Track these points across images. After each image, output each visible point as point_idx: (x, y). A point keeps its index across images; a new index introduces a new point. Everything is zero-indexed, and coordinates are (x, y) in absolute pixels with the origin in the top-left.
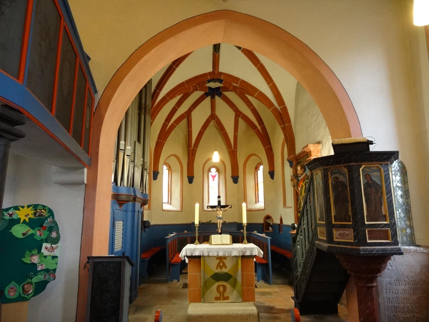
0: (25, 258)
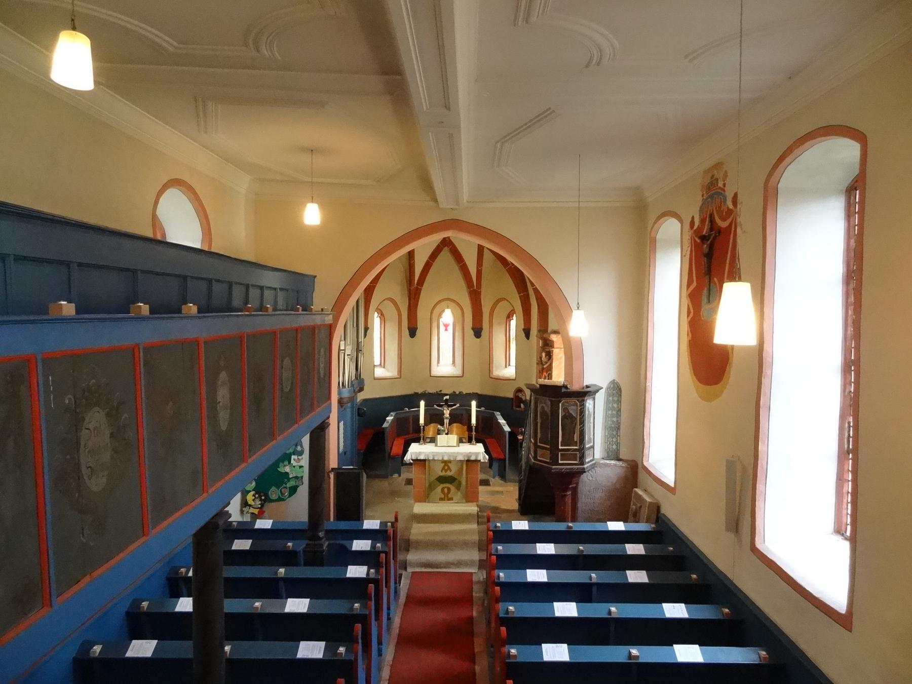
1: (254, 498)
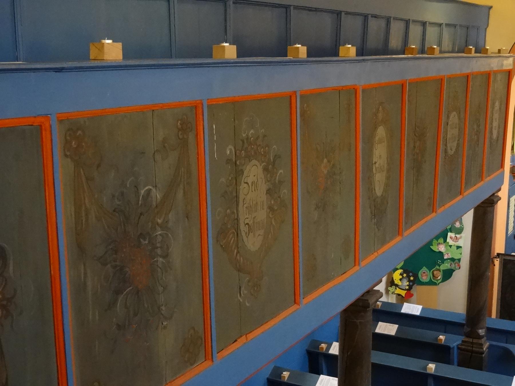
0: (433, 246)
1: (401, 277)
